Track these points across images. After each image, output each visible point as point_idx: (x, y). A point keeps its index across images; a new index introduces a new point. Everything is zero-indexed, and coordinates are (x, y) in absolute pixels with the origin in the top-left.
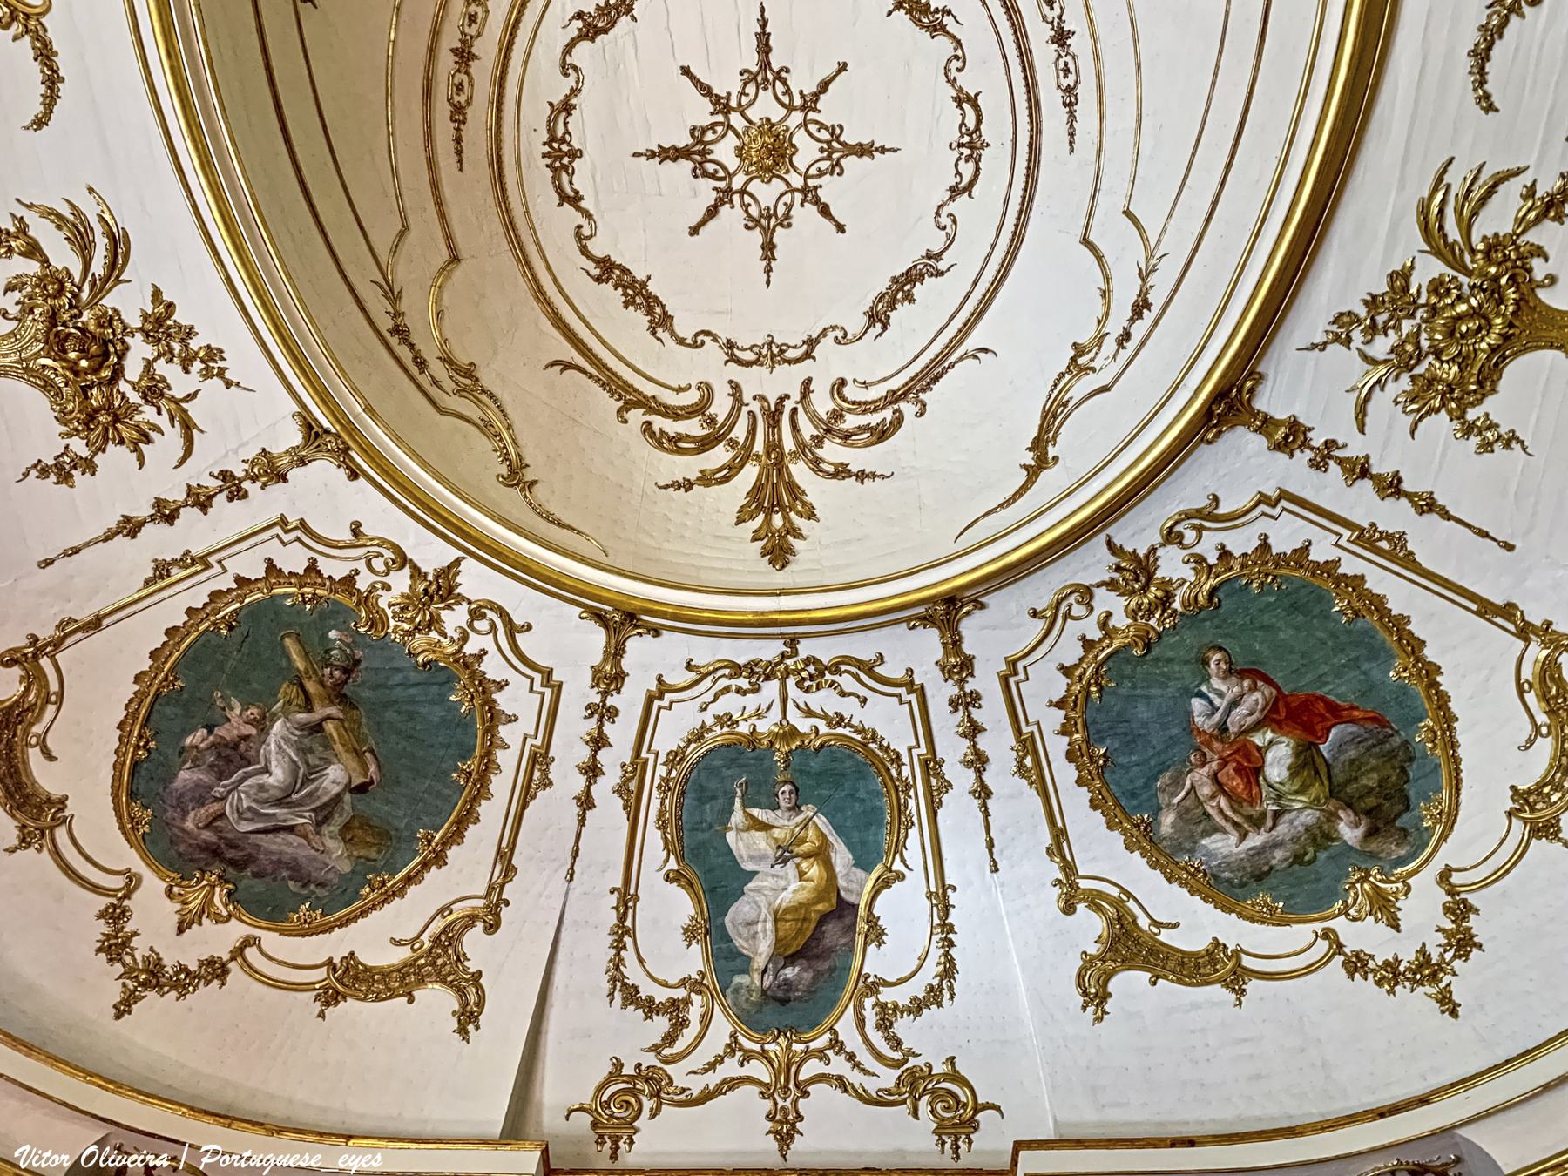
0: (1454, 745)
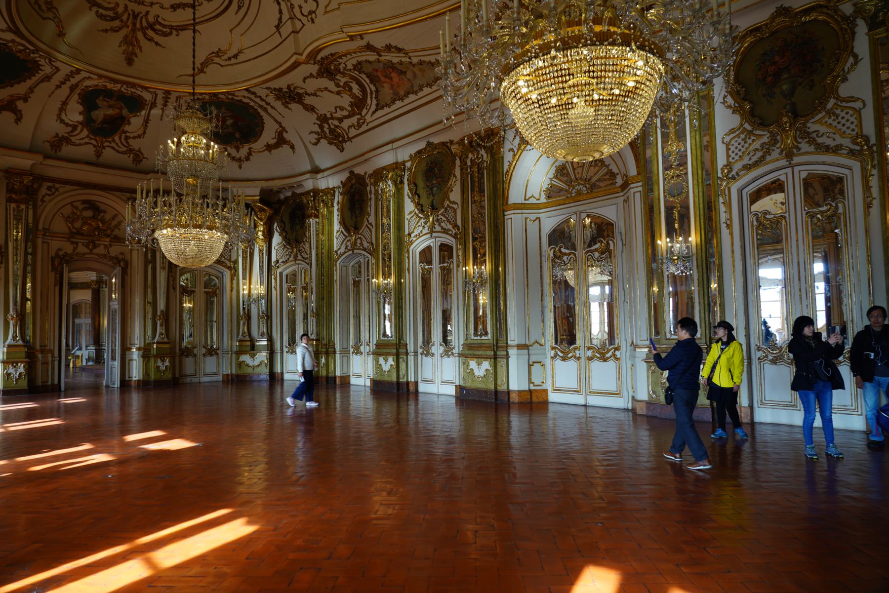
0: (262, 133)
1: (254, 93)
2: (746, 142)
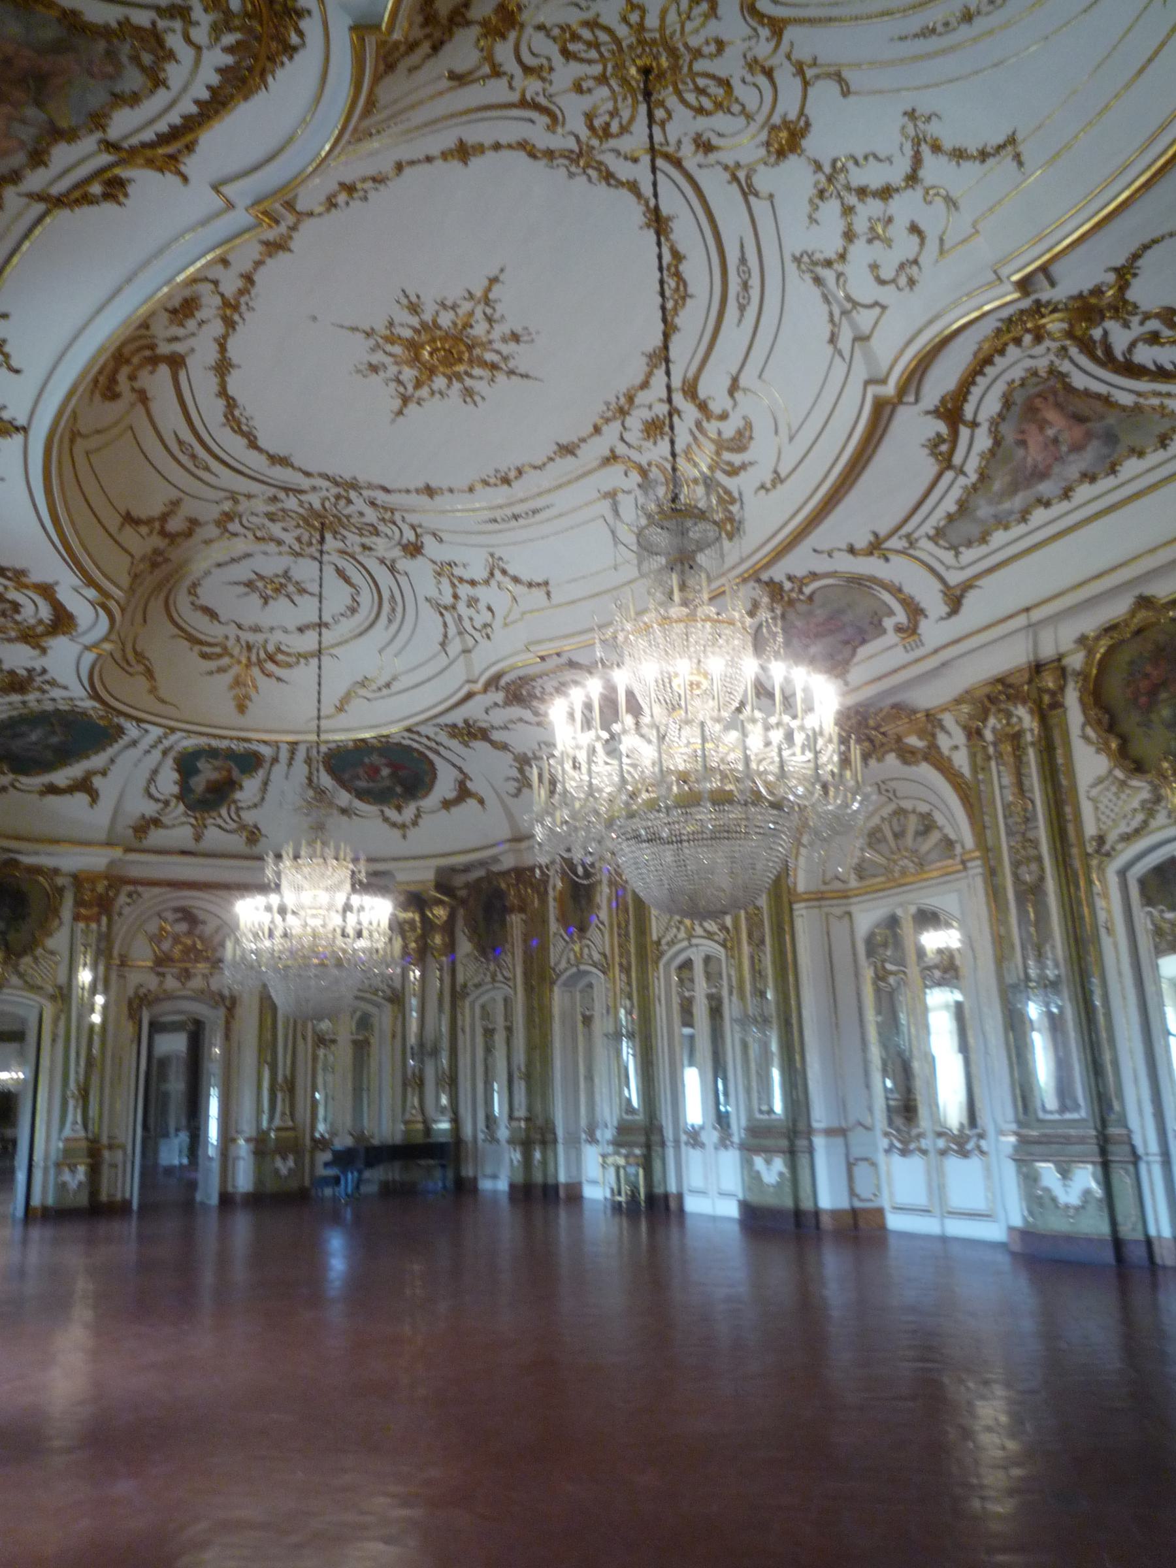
1: (418, 733)
2: (1118, 798)
